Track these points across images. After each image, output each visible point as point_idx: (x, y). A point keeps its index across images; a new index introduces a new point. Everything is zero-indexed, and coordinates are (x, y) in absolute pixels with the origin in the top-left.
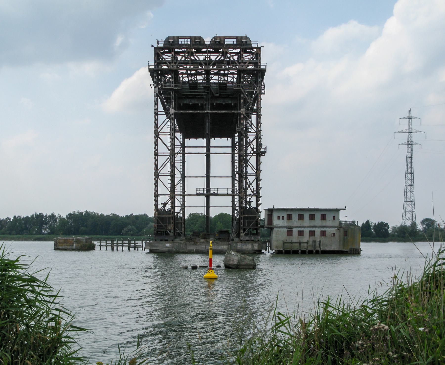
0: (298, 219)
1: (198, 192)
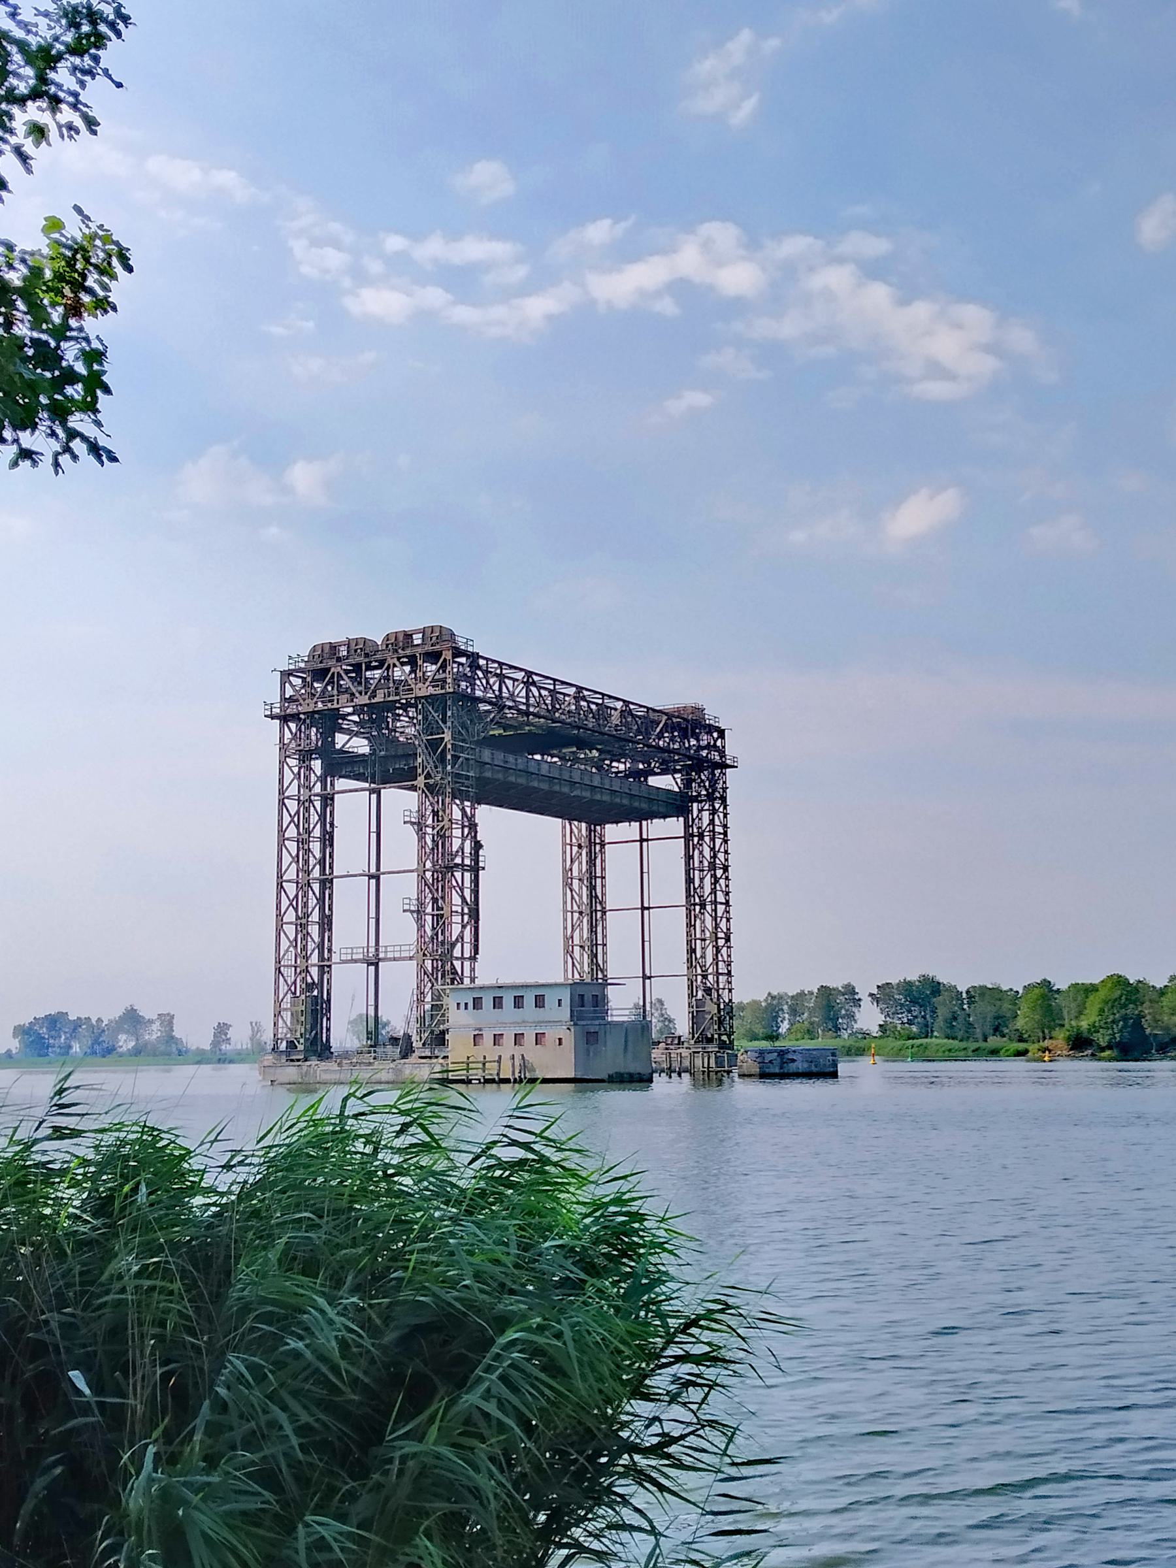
0: (494, 1008)
1: (344, 957)
